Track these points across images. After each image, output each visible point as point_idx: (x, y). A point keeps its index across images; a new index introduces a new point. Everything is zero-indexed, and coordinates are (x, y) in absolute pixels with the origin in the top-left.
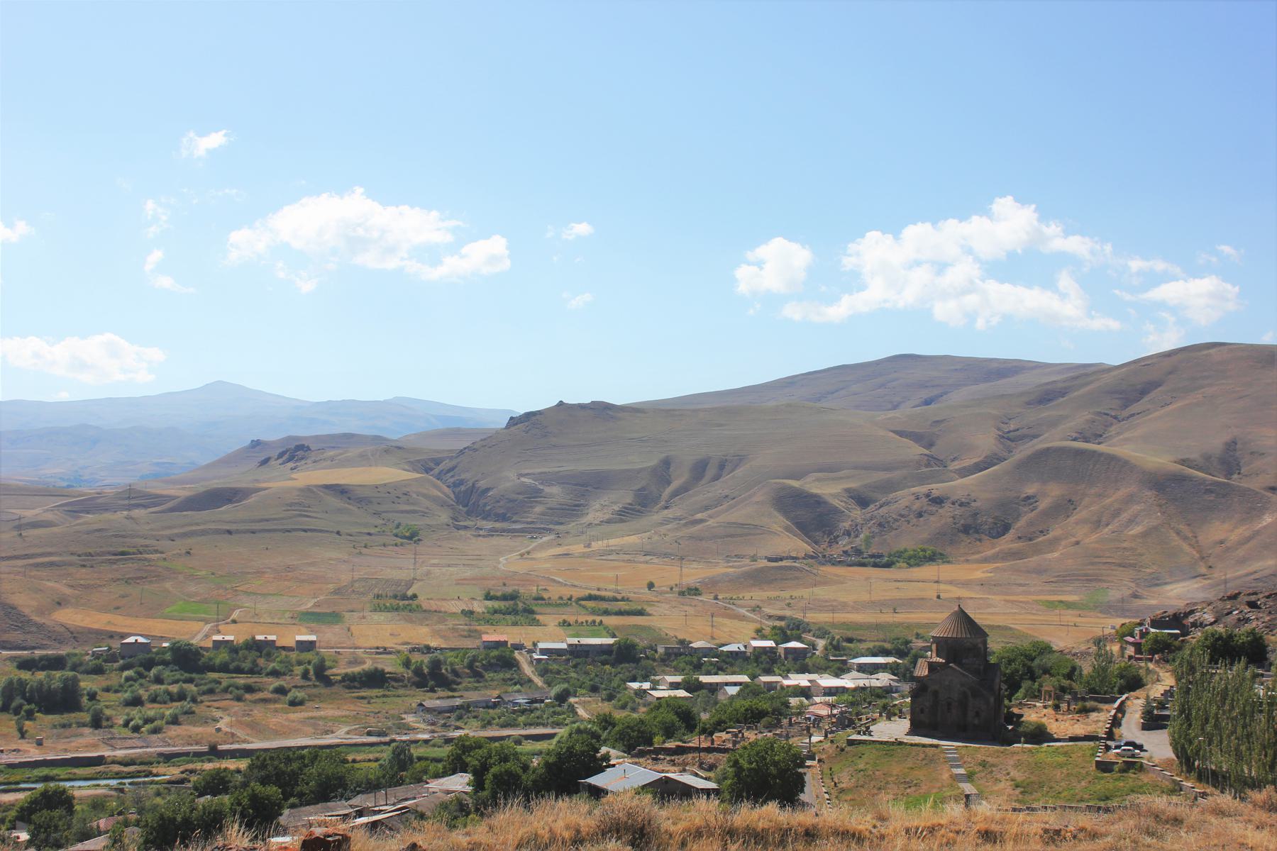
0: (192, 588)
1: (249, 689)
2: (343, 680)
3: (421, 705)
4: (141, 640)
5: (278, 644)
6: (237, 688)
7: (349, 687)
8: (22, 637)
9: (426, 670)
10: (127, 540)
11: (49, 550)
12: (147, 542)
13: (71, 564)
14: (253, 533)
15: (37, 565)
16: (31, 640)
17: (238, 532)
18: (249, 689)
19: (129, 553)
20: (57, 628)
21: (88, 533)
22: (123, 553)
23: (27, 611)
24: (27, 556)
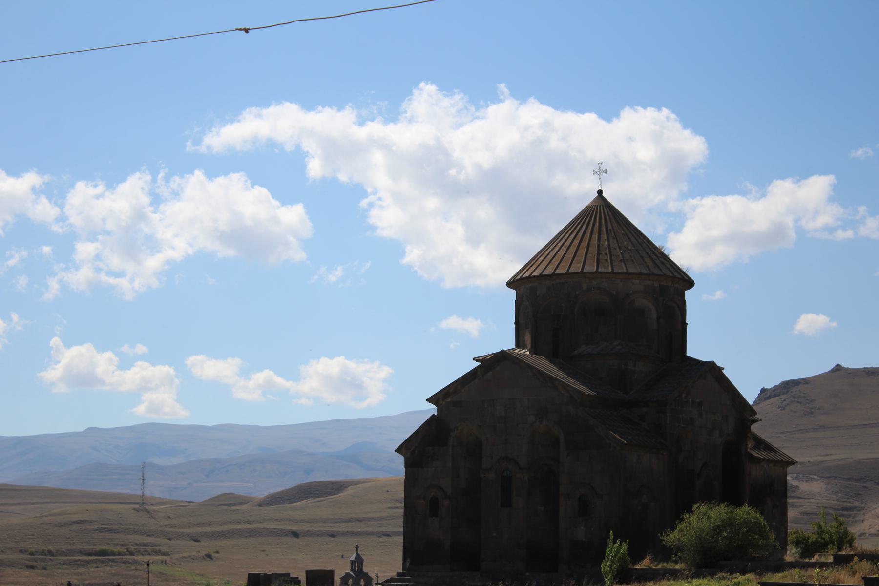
10: (118, 536)
12: (148, 540)
13: (11, 564)
14: (333, 536)
17: (308, 534)
19: (113, 554)
21: (61, 525)
22: (103, 553)
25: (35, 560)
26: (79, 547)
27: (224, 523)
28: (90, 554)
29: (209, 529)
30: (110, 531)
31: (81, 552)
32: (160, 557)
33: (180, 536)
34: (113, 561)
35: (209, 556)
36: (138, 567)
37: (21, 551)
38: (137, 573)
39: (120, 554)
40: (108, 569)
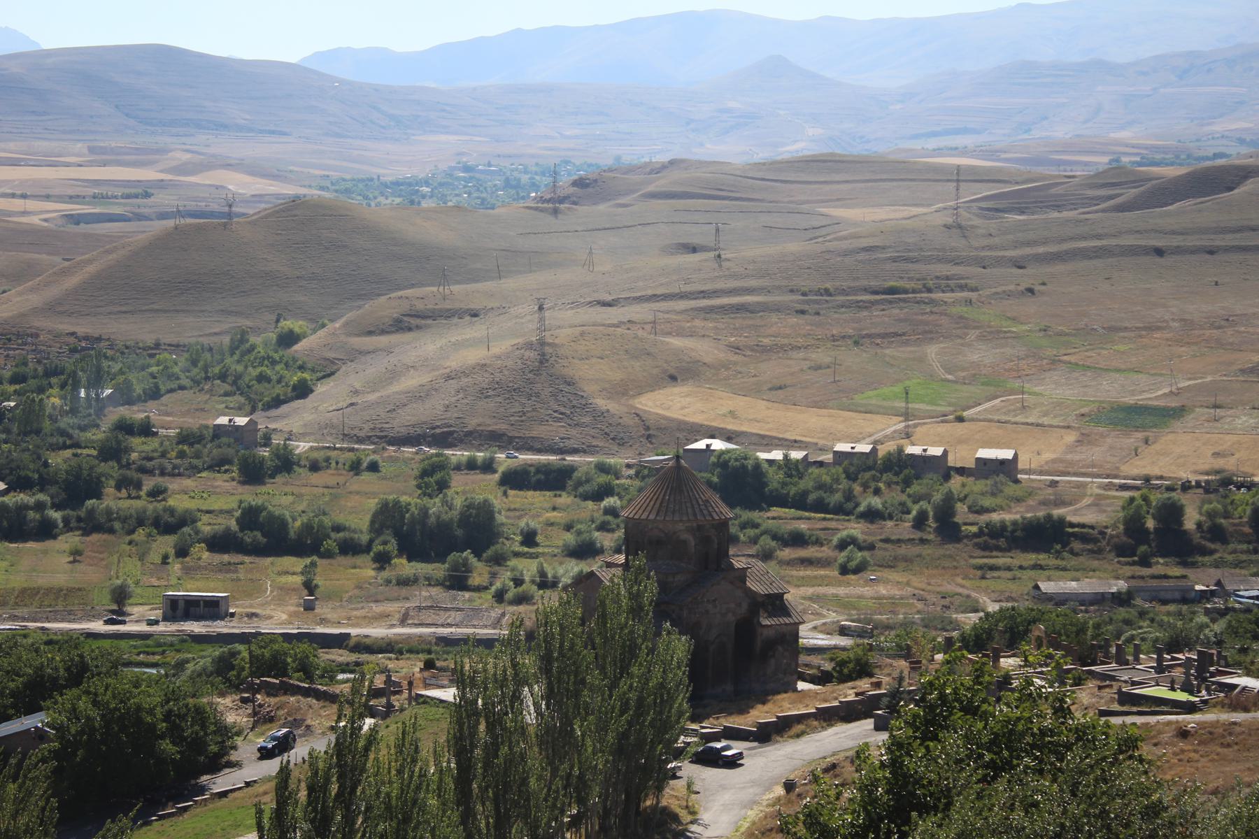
0: (980, 355)
1: (797, 540)
2: (981, 533)
3: (1037, 587)
4: (718, 445)
5: (952, 461)
6: (775, 537)
7: (985, 547)
8: (563, 432)
9: (1150, 524)
11: (753, 283)
13: (777, 309)
14: (1211, 252)
15: (711, 310)
16: (575, 437)
17: (1178, 251)
18: (797, 540)
19: (906, 291)
20: (629, 421)
21: (846, 253)
22: (892, 291)
23: (589, 389)
24: (703, 294)
25: (807, 302)
26: (865, 283)
27: (1063, 240)
28: (876, 293)
29: (1041, 250)
30: (907, 260)
31: (866, 290)
32: (965, 294)
33: (999, 262)
34: (904, 300)
35: (1031, 291)
36: (935, 309)
37: (792, 291)
38: (932, 318)
39: (914, 291)
40: (896, 311)
